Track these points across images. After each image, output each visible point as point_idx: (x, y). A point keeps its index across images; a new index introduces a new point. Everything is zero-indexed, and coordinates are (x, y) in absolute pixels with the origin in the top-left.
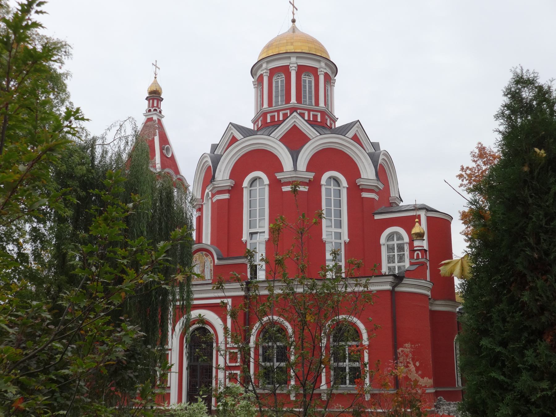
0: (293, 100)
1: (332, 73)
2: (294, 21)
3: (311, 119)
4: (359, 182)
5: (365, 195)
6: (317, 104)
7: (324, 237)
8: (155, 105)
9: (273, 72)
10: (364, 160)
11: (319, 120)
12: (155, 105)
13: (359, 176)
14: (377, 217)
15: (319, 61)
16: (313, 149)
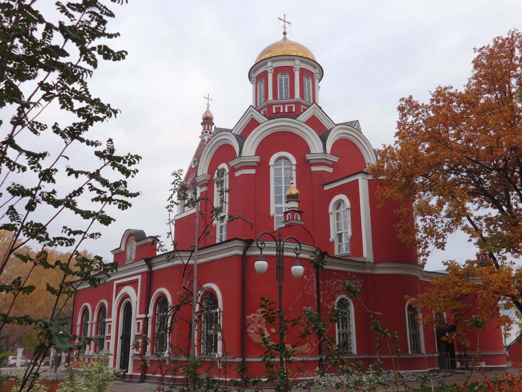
0: (270, 97)
1: (315, 68)
2: (285, 33)
3: (286, 111)
4: (308, 157)
5: (314, 169)
6: (292, 95)
7: (272, 212)
8: (206, 128)
9: (258, 78)
10: (311, 137)
11: (294, 111)
12: (206, 128)
13: (309, 152)
14: (326, 188)
15: (294, 60)
16: (261, 134)
